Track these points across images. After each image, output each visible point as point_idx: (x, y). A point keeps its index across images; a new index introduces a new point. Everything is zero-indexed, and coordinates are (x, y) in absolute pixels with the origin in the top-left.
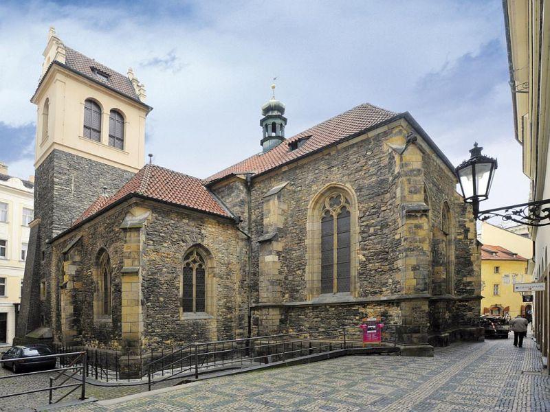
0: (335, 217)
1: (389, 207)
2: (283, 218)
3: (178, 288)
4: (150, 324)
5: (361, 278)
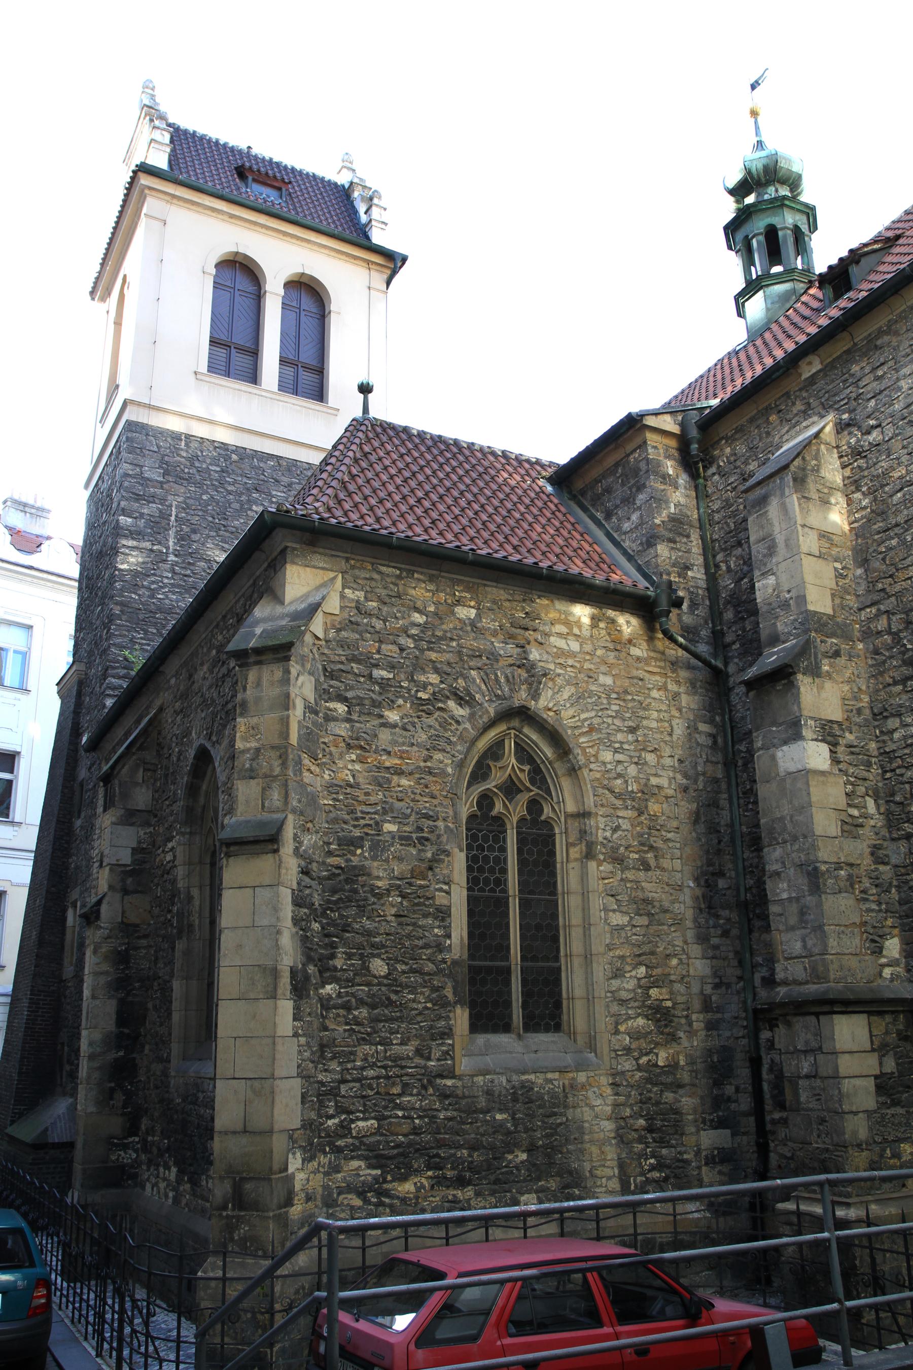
3: (443, 914)
4: (333, 1093)
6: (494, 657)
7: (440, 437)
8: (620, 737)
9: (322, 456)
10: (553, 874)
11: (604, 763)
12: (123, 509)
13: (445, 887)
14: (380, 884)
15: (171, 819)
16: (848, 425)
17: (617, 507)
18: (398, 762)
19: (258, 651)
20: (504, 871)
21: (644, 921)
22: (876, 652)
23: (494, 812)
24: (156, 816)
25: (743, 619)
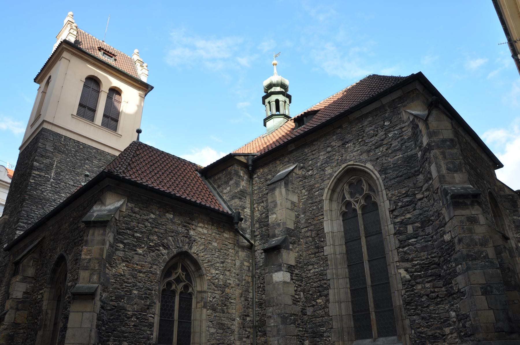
0: (359, 212)
1: (426, 194)
2: (293, 215)
3: (151, 325)
5: (409, 310)
6: (178, 233)
7: (163, 152)
8: (218, 265)
9: (119, 153)
10: (190, 313)
11: (212, 274)
12: (36, 160)
13: (153, 316)
14: (129, 313)
15: (43, 281)
16: (302, 168)
17: (222, 184)
18: (140, 267)
19: (94, 222)
20: (173, 311)
21: (221, 331)
22: (306, 243)
23: (172, 289)
24: (35, 280)
25: (262, 227)
